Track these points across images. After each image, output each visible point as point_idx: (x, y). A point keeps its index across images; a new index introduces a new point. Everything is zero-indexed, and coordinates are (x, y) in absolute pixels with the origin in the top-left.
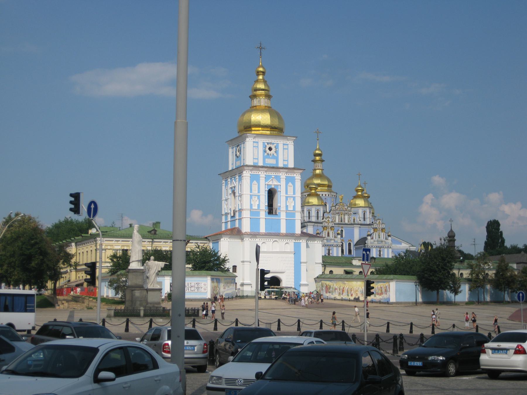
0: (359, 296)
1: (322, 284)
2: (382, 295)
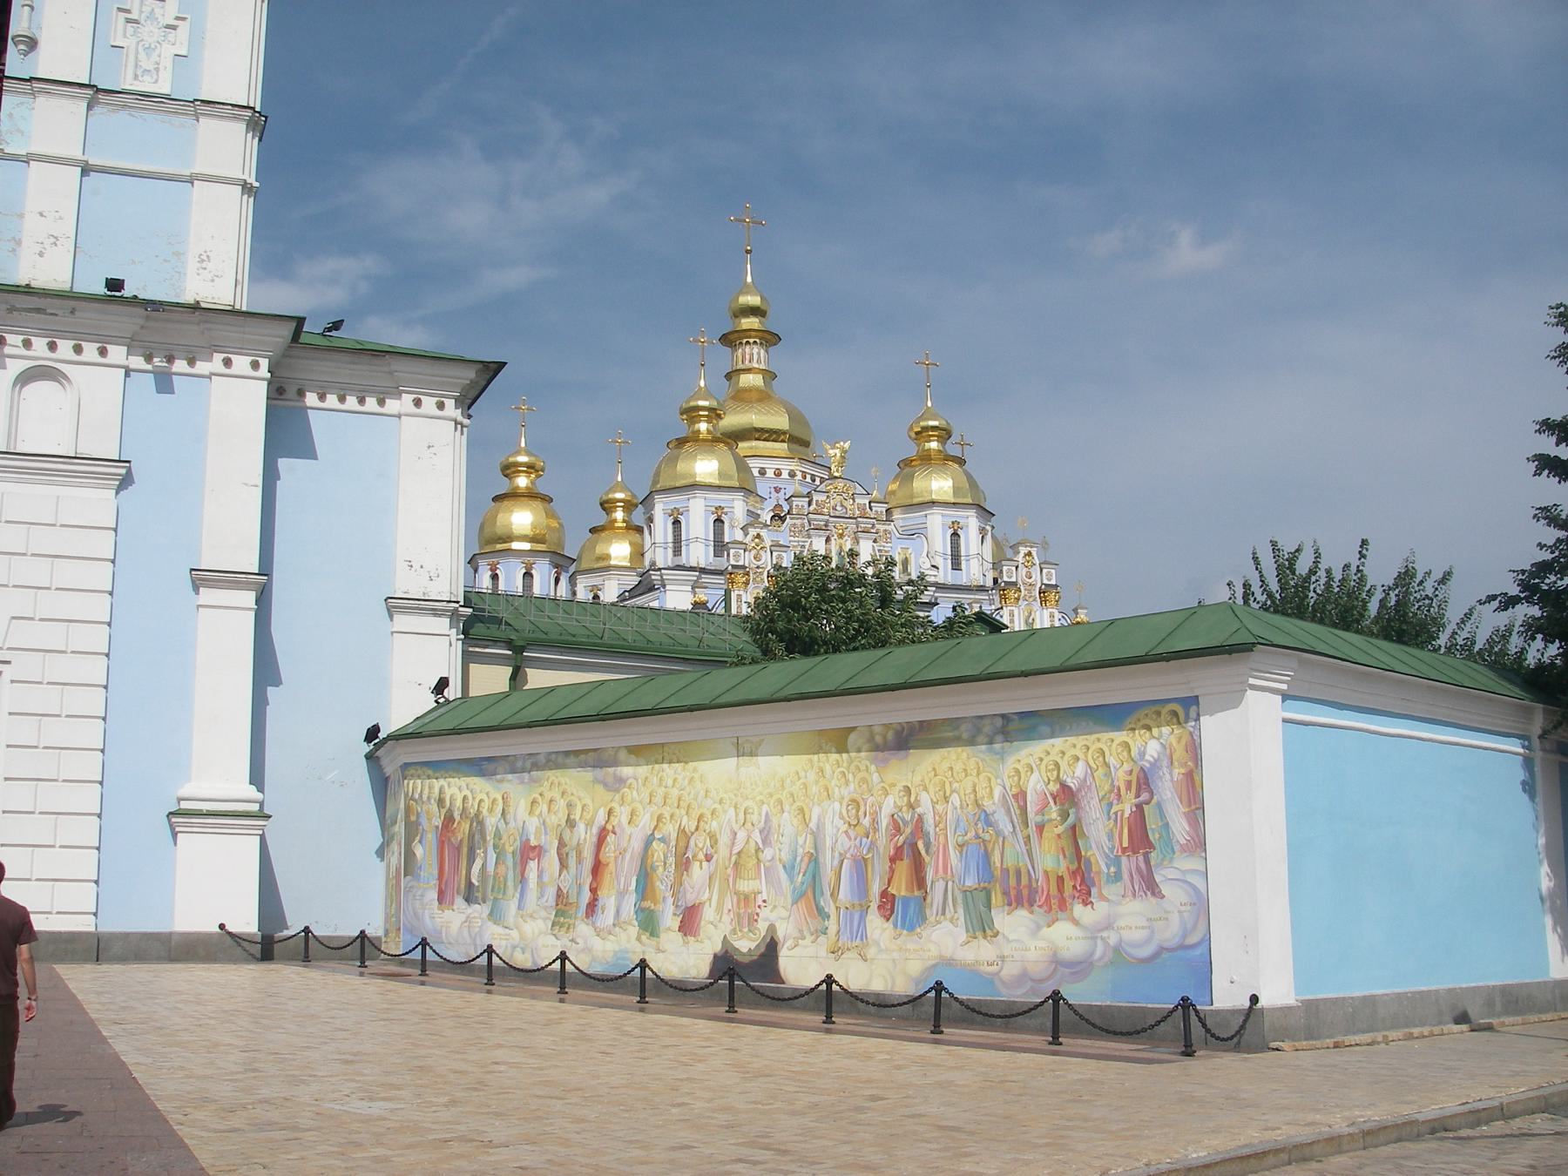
0: (772, 928)
1: (408, 810)
2: (1078, 909)
